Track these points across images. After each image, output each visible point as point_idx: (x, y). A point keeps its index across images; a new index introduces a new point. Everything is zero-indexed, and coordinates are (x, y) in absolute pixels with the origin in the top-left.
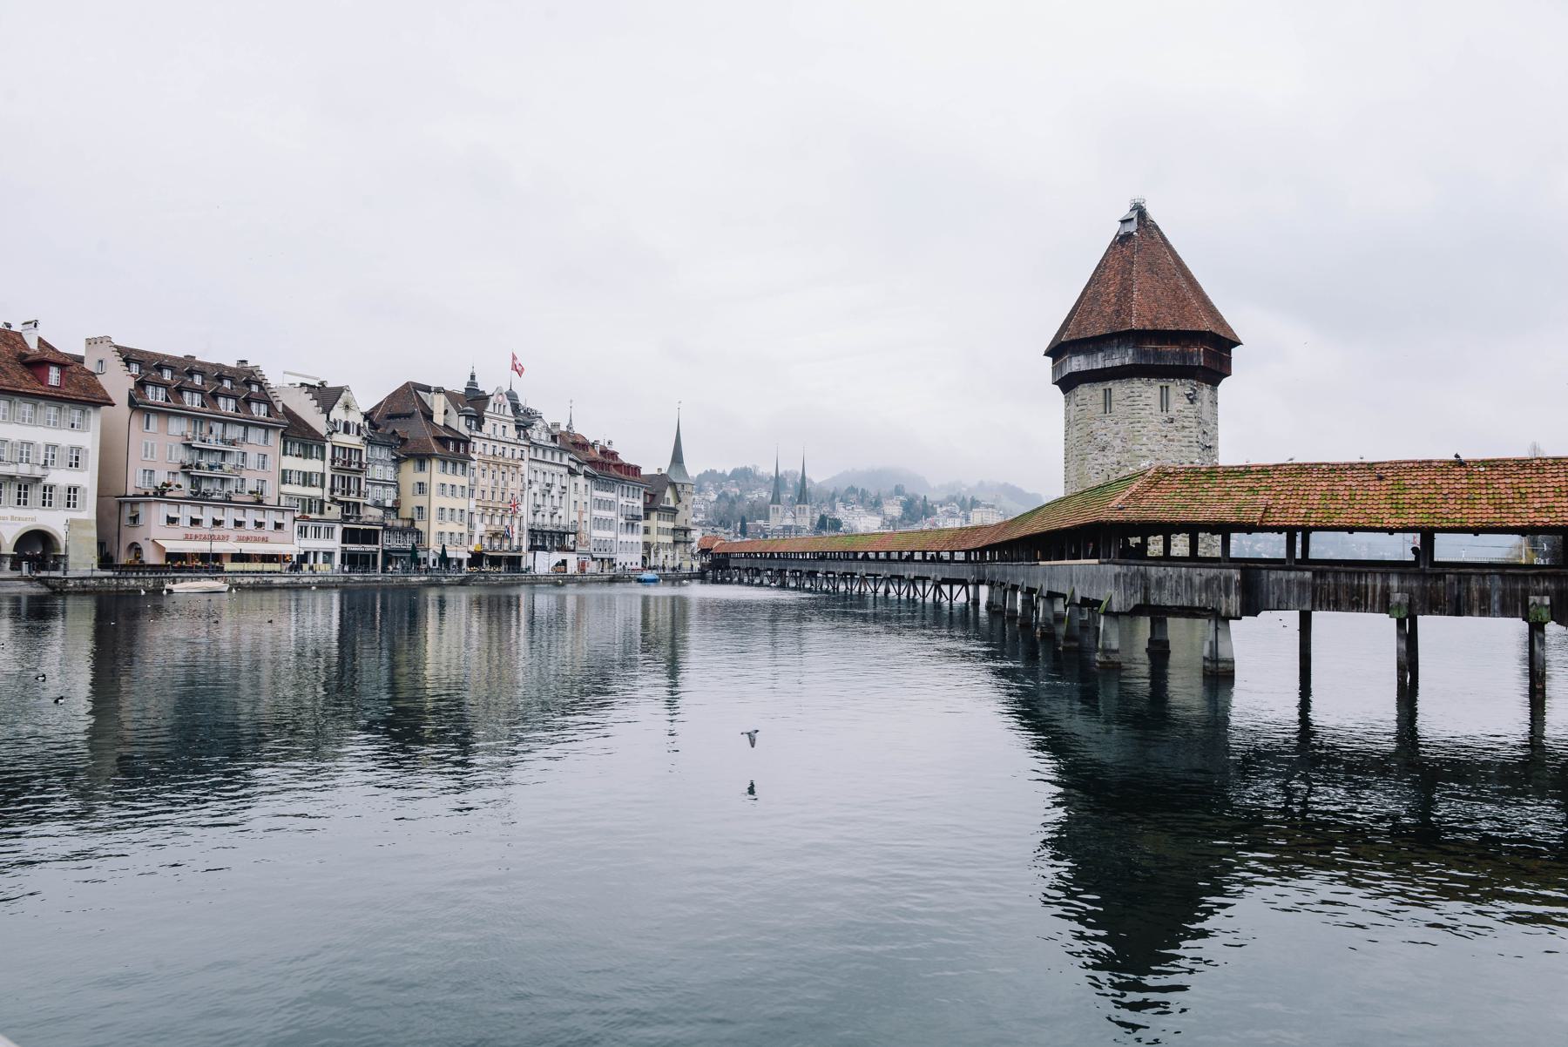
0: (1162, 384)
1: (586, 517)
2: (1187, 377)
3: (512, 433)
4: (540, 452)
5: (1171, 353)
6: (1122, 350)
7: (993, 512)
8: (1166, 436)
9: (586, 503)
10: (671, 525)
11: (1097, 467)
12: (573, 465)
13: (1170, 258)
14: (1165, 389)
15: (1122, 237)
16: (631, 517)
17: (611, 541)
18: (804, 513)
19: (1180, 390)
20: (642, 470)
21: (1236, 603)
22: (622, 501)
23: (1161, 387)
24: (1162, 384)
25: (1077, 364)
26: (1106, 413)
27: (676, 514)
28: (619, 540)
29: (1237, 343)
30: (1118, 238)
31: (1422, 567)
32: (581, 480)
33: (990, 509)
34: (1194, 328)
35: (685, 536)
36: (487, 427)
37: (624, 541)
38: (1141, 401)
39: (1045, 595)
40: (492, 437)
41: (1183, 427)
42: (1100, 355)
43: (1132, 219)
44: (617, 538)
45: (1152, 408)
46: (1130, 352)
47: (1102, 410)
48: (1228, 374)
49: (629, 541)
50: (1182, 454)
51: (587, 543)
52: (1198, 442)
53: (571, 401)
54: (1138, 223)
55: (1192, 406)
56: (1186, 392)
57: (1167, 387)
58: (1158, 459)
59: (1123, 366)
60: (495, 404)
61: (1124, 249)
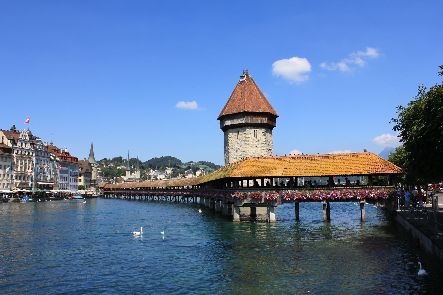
3: (28, 146)
4: (39, 153)
5: (257, 120)
7: (204, 172)
8: (257, 146)
10: (89, 179)
13: (256, 89)
14: (255, 131)
18: (138, 173)
20: (78, 159)
22: (71, 170)
23: (255, 130)
25: (228, 123)
28: (70, 184)
29: (277, 117)
30: (240, 82)
33: (203, 171)
34: (264, 112)
36: (19, 144)
37: (71, 184)
38: (248, 135)
39: (217, 201)
40: (21, 147)
41: (262, 143)
42: (235, 120)
43: (244, 76)
45: (252, 137)
48: (276, 126)
49: (74, 185)
50: (262, 152)
52: (266, 148)
53: (52, 134)
54: (246, 77)
55: (264, 136)
57: (256, 130)
58: (254, 154)
59: (242, 123)
60: (22, 136)
61: (242, 85)
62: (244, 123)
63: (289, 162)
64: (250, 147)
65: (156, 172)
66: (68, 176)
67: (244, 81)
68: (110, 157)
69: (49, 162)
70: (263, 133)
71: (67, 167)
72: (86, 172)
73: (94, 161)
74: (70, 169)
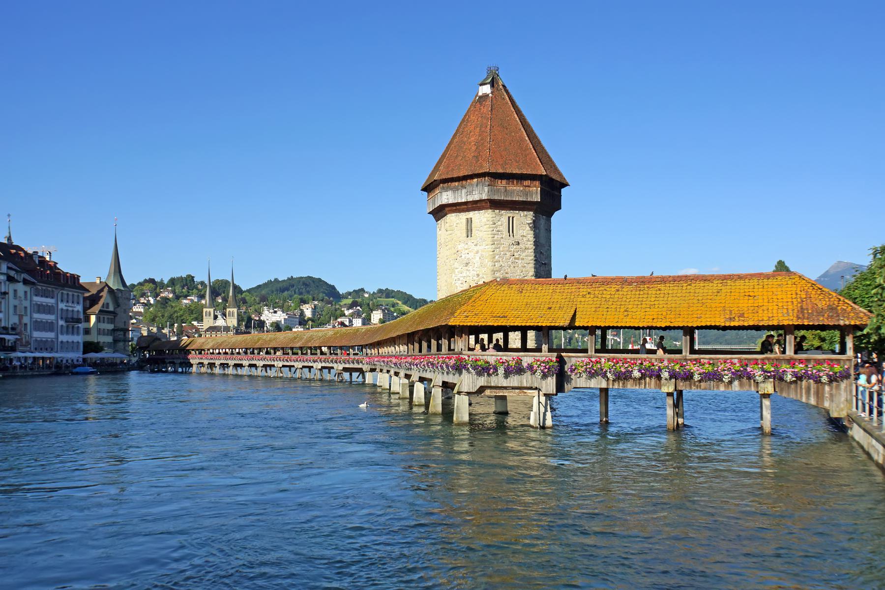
0: (511, 215)
1: (26, 320)
2: (529, 210)
5: (516, 192)
6: (480, 187)
9: (26, 308)
10: (111, 327)
11: (461, 279)
12: (12, 273)
13: (516, 116)
14: (511, 219)
15: (481, 97)
16: (71, 320)
17: (52, 341)
19: (523, 220)
21: (553, 383)
22: (62, 306)
23: (509, 218)
24: (511, 215)
25: (446, 197)
26: (468, 237)
27: (115, 317)
28: (60, 340)
29: (565, 185)
31: (684, 353)
32: (21, 288)
35: (125, 335)
37: (65, 340)
42: (464, 191)
44: (57, 339)
46: (486, 189)
47: (465, 235)
48: (559, 208)
49: (70, 341)
51: (28, 343)
56: (528, 222)
57: (513, 218)
58: (507, 273)
61: (482, 107)
62: (485, 200)
63: (589, 293)
64: (497, 257)
65: (275, 312)
66: (54, 319)
67: (488, 95)
68: (163, 276)
69: (5, 284)
70: (528, 223)
71: (52, 298)
72: (100, 311)
73: (121, 285)
74: (59, 303)
